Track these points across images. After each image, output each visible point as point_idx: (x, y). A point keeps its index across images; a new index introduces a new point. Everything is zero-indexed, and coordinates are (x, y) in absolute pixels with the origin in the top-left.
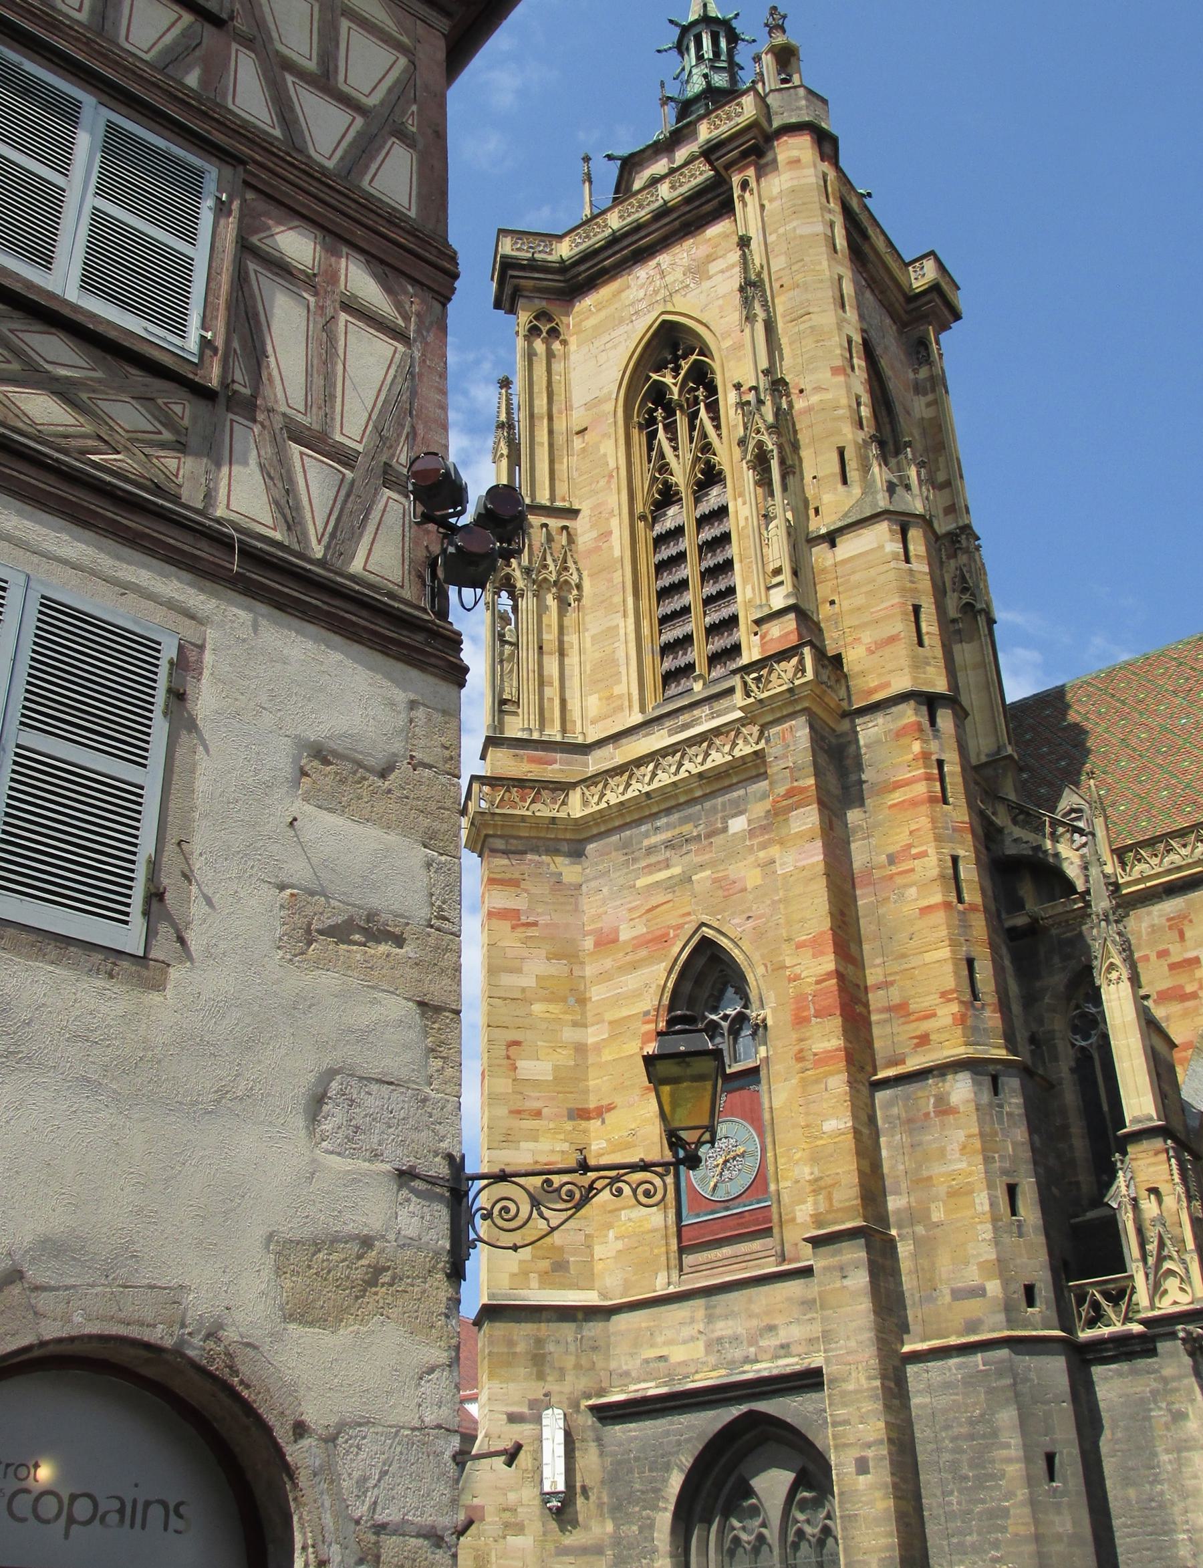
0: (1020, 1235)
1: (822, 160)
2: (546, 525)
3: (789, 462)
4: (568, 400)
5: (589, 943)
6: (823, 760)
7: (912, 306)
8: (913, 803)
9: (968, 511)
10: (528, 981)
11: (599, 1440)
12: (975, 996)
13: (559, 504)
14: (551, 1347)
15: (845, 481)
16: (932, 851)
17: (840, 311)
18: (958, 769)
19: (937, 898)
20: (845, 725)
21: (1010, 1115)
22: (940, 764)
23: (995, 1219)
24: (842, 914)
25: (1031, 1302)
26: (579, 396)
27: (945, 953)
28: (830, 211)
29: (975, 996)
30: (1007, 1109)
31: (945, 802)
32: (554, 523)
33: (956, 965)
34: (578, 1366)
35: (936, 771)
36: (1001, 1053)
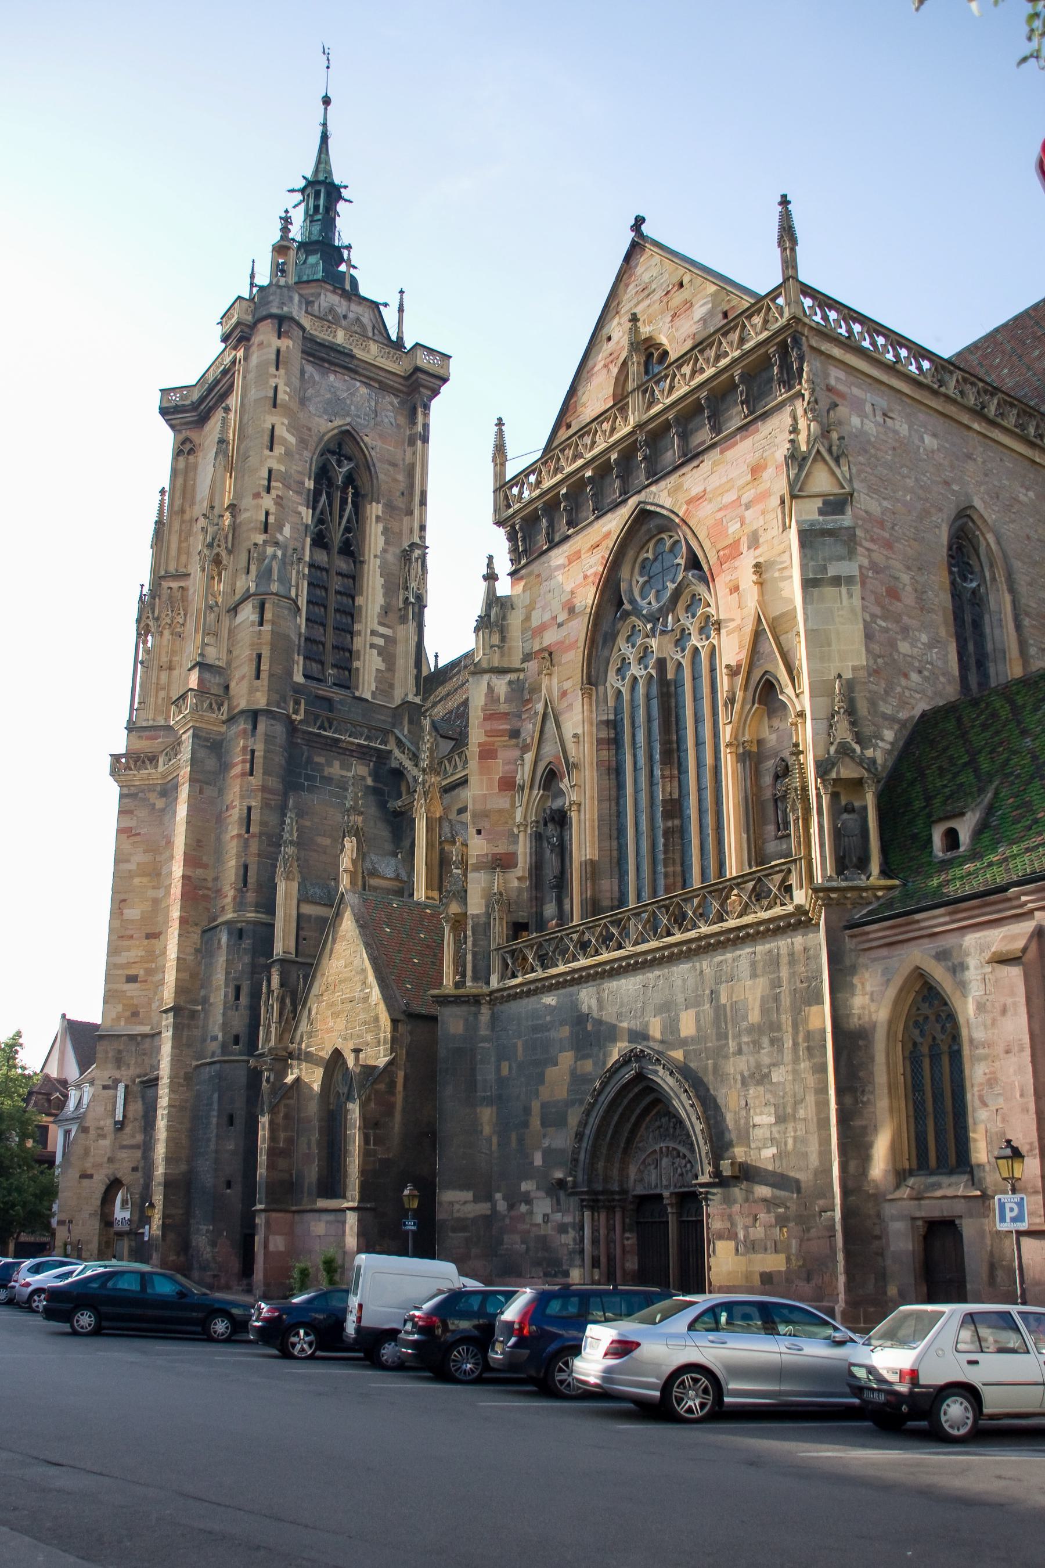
0: (237, 1010)
1: (279, 338)
2: (171, 588)
3: (225, 562)
4: (193, 497)
5: (164, 843)
6: (202, 753)
7: (410, 381)
8: (236, 776)
9: (423, 528)
10: (132, 866)
11: (143, 1098)
12: (245, 886)
13: (182, 570)
14: (124, 1054)
15: (248, 573)
16: (237, 803)
17: (267, 452)
18: (262, 753)
19: (235, 832)
20: (223, 729)
21: (245, 949)
22: (253, 752)
23: (225, 1003)
24: (199, 841)
25: (236, 1042)
26: (198, 498)
27: (233, 863)
28: (276, 376)
29: (245, 886)
30: (243, 946)
31: (251, 774)
32: (175, 585)
33: (237, 869)
34: (136, 1063)
35: (249, 757)
36: (251, 915)
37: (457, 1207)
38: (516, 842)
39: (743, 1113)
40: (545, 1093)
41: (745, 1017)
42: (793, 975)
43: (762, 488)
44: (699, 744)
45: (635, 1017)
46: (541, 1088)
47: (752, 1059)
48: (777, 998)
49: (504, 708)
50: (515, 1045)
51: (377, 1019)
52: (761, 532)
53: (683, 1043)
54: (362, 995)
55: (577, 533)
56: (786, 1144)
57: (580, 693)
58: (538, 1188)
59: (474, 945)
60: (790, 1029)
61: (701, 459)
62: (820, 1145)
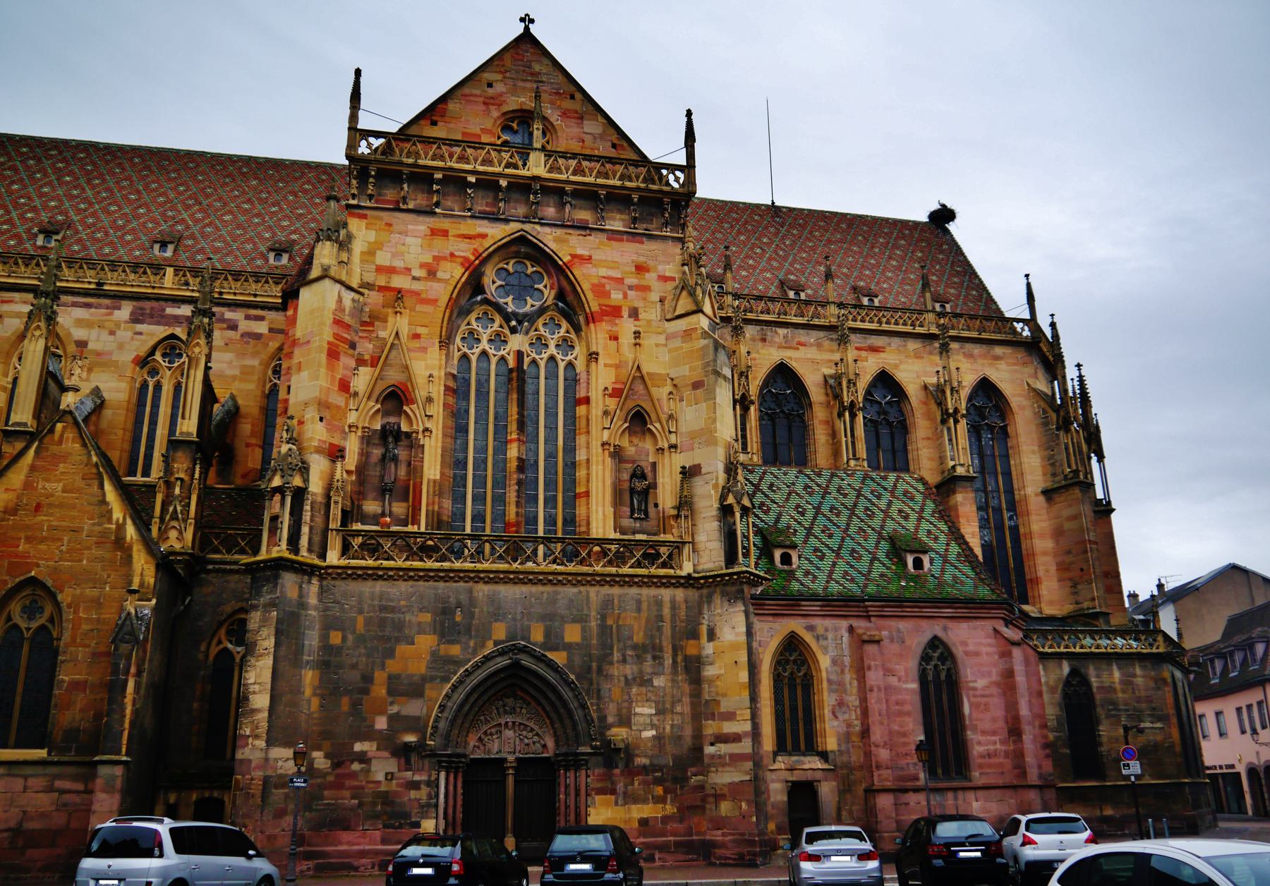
37: (280, 763)
38: (345, 439)
39: (626, 704)
40: (393, 666)
41: (631, 638)
42: (673, 616)
43: (644, 283)
44: (551, 428)
45: (514, 619)
46: (389, 662)
47: (635, 667)
48: (659, 629)
49: (347, 319)
50: (354, 620)
51: (128, 560)
52: (640, 311)
53: (569, 647)
54: (97, 528)
55: (445, 216)
56: (664, 729)
57: (437, 344)
58: (378, 749)
59: (312, 520)
60: (670, 651)
61: (588, 232)
62: (693, 731)
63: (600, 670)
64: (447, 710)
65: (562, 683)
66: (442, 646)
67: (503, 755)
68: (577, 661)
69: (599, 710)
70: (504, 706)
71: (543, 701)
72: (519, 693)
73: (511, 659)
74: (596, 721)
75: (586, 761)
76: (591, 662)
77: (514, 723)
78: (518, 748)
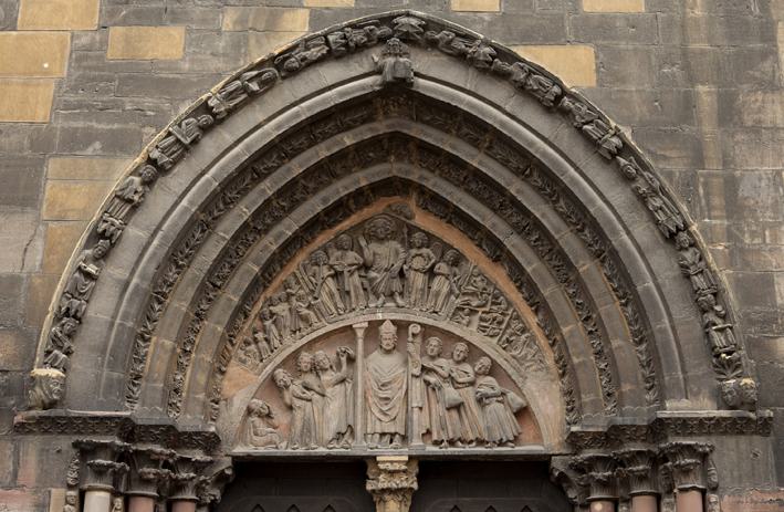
63: (728, 112)
64: (124, 256)
65: (579, 152)
66: (117, 32)
67: (358, 448)
68: (638, 86)
69: (737, 254)
70: (366, 267)
71: (514, 243)
72: (424, 221)
73: (379, 71)
74: (731, 296)
75: (704, 456)
76: (692, 80)
77: (401, 326)
78: (420, 422)
